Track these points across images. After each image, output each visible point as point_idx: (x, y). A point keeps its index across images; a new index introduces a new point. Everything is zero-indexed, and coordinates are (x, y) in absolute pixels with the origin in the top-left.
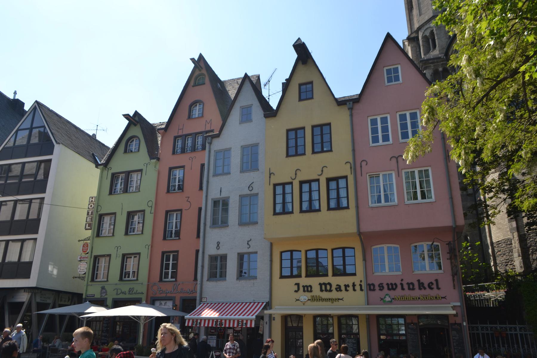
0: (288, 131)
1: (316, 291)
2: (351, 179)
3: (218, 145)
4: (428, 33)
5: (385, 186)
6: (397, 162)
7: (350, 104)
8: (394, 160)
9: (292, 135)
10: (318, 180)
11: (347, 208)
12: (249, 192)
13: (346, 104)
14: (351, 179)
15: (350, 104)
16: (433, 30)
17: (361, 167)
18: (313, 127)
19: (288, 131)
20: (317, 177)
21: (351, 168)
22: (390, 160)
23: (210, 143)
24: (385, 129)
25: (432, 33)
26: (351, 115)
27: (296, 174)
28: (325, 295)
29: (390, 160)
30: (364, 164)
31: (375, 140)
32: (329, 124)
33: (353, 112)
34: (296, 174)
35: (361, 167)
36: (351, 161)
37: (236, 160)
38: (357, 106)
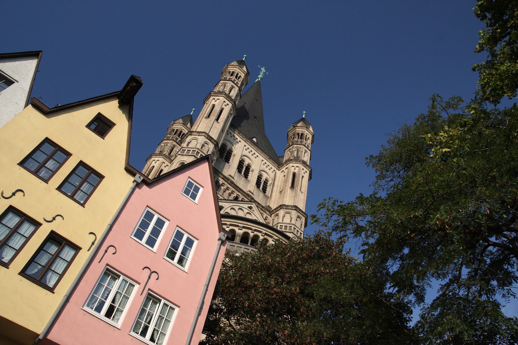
0: (47, 140)
2: (83, 257)
5: (118, 295)
6: (149, 277)
7: (140, 177)
8: (147, 272)
9: (48, 149)
10: (37, 224)
11: (51, 290)
13: (134, 175)
14: (83, 257)
15: (140, 177)
17: (106, 251)
18: (81, 164)
19: (47, 140)
20: (41, 221)
21: (93, 243)
22: (143, 269)
24: (156, 232)
27: (14, 194)
29: (143, 269)
30: (111, 250)
31: (139, 235)
32: (101, 177)
33: (137, 189)
34: (14, 194)
35: (106, 251)
36: (100, 236)
38: (145, 187)
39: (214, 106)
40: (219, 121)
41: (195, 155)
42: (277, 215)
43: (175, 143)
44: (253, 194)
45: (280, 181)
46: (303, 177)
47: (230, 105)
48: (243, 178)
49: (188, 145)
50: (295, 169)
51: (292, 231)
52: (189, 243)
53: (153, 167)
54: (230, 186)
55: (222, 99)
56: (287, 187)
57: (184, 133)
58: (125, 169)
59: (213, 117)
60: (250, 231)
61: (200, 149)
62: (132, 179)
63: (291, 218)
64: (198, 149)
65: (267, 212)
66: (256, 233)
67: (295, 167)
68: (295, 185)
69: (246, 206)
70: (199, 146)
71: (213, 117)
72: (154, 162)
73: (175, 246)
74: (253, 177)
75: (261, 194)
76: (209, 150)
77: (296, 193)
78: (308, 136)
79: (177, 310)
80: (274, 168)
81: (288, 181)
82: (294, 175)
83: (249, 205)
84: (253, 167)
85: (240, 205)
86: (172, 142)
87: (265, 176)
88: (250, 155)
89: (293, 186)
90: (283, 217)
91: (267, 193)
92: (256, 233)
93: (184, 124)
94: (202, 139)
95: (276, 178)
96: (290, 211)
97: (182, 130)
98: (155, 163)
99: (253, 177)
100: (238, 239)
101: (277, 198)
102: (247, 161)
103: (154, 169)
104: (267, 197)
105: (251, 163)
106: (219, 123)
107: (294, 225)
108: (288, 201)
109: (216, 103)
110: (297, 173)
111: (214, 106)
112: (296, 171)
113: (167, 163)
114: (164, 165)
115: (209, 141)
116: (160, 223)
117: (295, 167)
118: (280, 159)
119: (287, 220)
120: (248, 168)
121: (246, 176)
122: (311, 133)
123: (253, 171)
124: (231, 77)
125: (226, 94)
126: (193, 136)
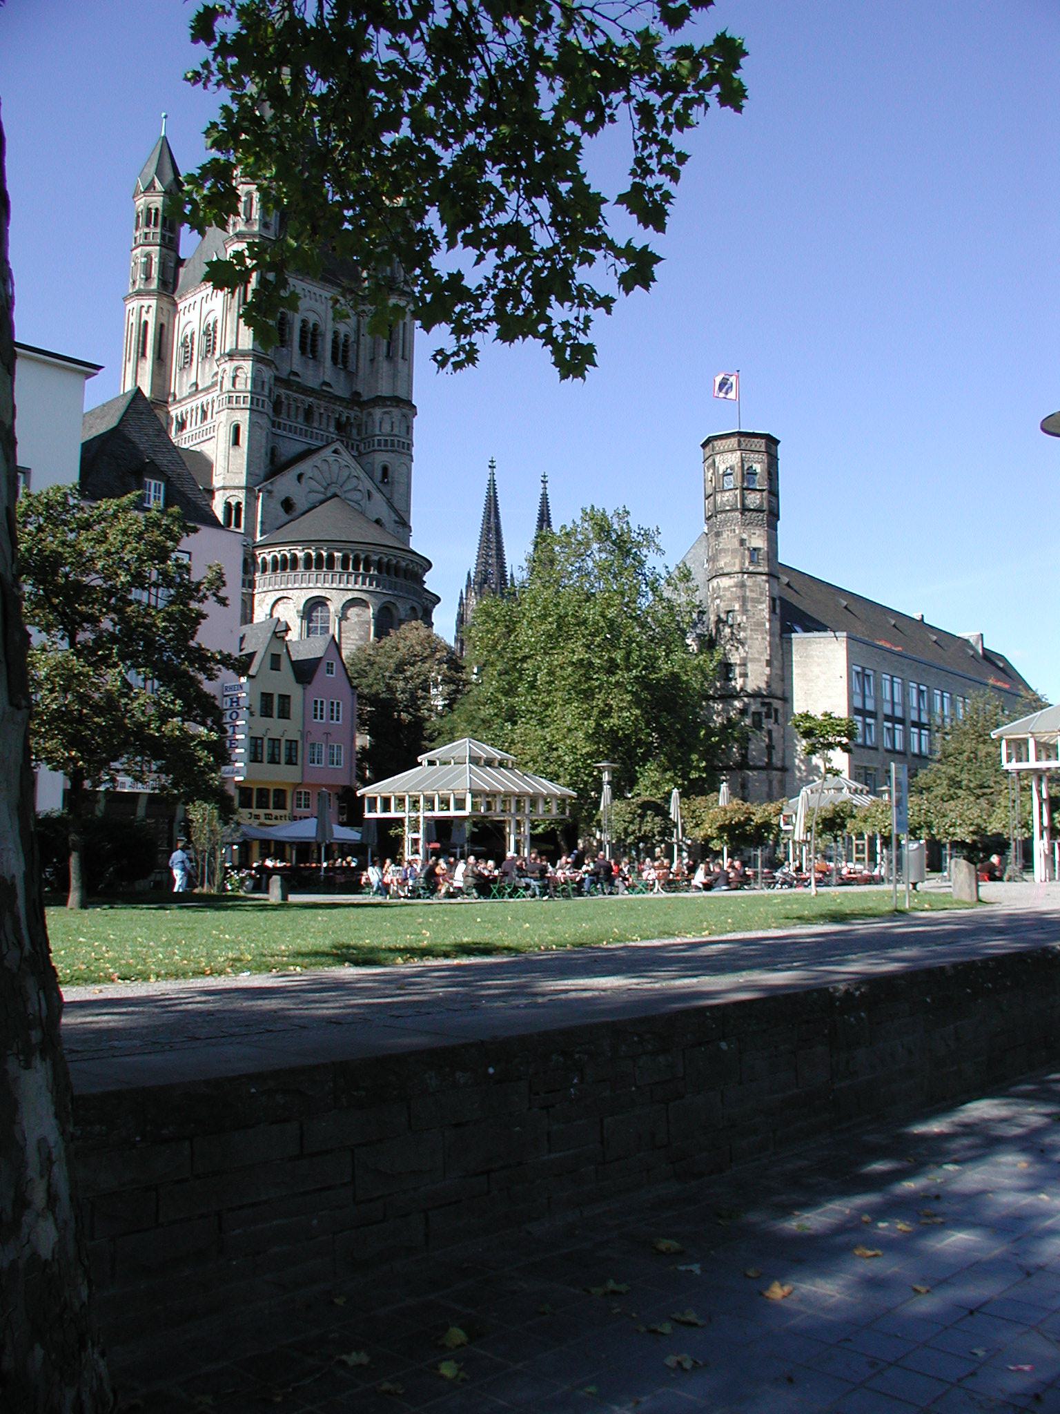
1: (262, 817)
4: (233, 502)
10: (279, 740)
11: (296, 764)
24: (322, 710)
25: (239, 504)
26: (304, 694)
28: (268, 822)
31: (316, 718)
38: (309, 687)
41: (248, 406)
42: (370, 414)
48: (311, 362)
53: (146, 323)
54: (296, 395)
56: (381, 358)
63: (393, 423)
75: (342, 374)
84: (322, 328)
91: (352, 367)
96: (391, 409)
98: (147, 312)
104: (351, 375)
105: (318, 319)
107: (396, 436)
108: (384, 389)
121: (314, 351)
123: (323, 335)
126: (236, 363)
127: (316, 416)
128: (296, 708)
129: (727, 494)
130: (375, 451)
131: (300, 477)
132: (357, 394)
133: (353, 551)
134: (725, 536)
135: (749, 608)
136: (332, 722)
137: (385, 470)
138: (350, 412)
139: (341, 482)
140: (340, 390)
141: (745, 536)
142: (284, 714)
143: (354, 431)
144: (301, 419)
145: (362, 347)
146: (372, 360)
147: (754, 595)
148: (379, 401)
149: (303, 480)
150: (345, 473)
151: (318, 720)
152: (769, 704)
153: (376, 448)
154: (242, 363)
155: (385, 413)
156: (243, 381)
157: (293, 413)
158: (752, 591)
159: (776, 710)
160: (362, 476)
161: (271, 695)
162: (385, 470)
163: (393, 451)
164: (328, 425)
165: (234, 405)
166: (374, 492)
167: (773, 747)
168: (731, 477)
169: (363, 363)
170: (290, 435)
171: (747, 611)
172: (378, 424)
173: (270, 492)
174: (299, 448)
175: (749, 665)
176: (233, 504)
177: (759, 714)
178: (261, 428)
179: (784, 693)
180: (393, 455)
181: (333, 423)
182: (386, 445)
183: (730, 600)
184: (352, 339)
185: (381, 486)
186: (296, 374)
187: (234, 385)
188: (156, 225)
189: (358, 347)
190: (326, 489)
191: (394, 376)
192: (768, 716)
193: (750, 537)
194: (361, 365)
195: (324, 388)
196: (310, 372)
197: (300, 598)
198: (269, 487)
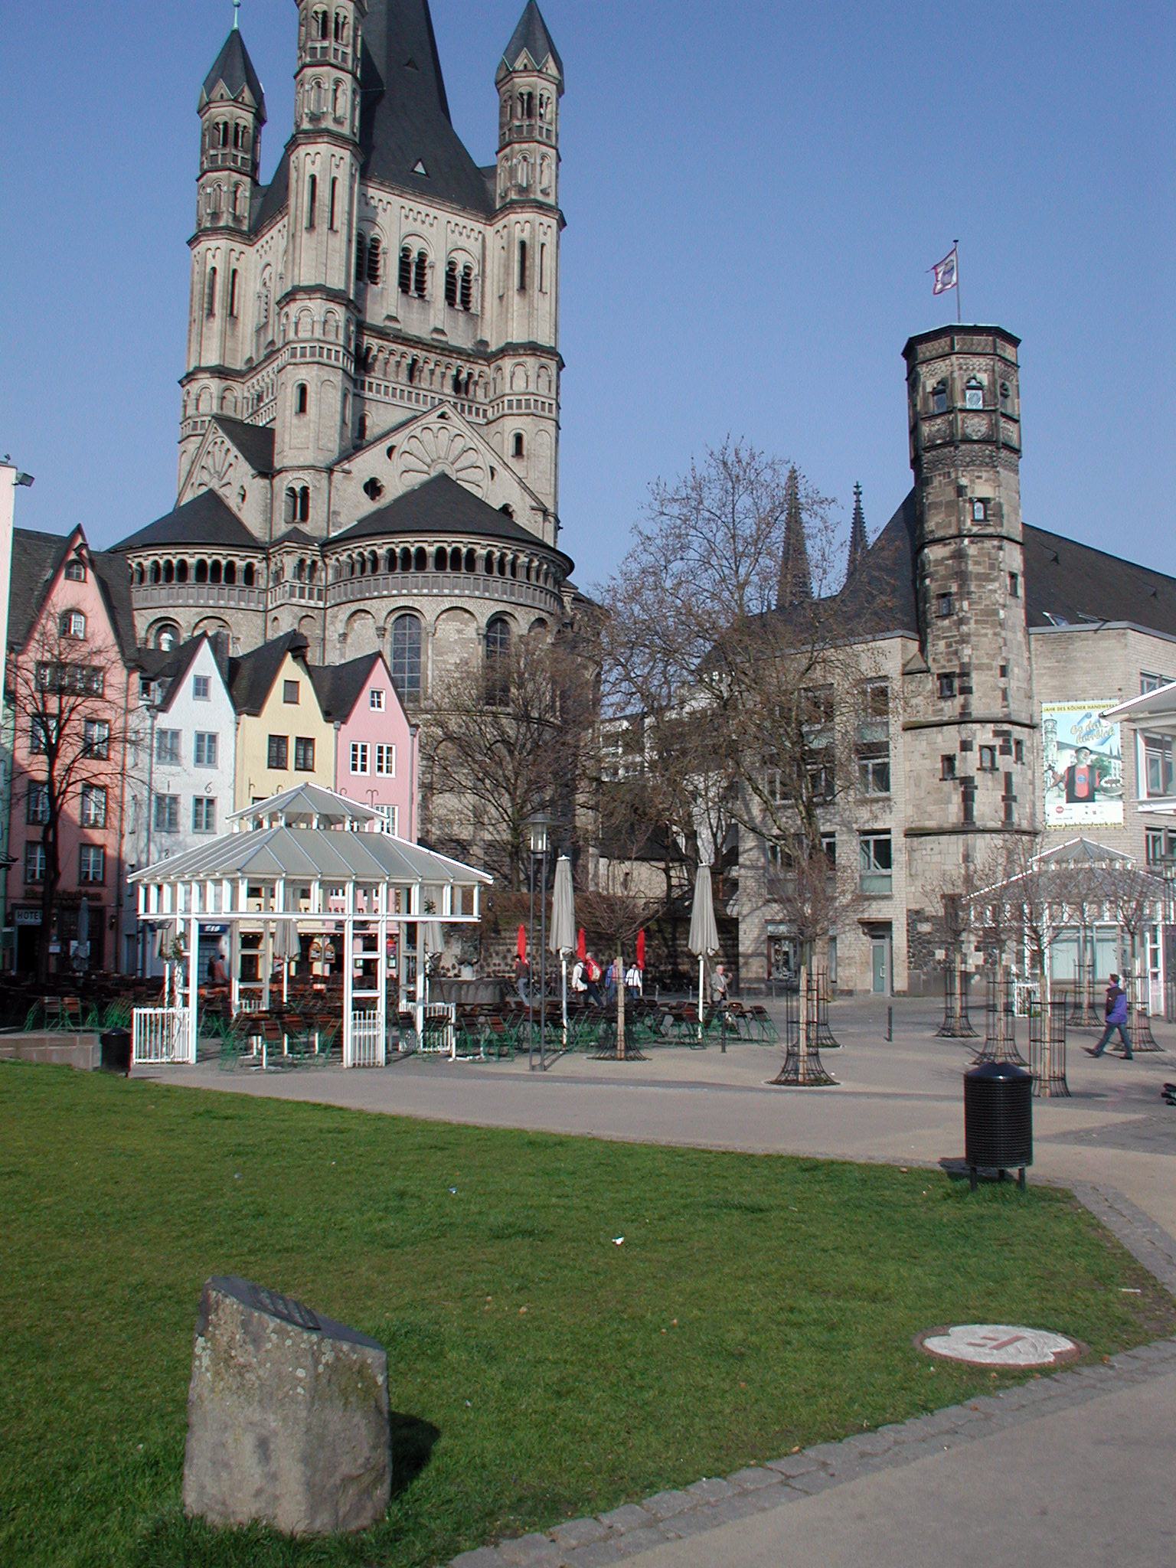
3: (164, 721)
12: (206, 794)
16: (307, 488)
23: (154, 718)
24: (364, 758)
25: (305, 490)
26: (337, 737)
31: (354, 768)
37: (187, 747)
39: (313, 178)
40: (337, 225)
42: (500, 369)
43: (236, 176)
44: (442, 332)
45: (496, 267)
46: (543, 245)
47: (347, 154)
48: (417, 303)
49: (296, 333)
50: (523, 231)
51: (532, 410)
52: (389, 750)
53: (214, 270)
54: (394, 346)
55: (323, 148)
56: (510, 293)
57: (245, 127)
58: (326, 721)
59: (322, 226)
60: (445, 545)
61: (322, 338)
62: (332, 725)
64: (319, 340)
65: (480, 362)
66: (454, 545)
67: (522, 222)
68: (528, 280)
69: (433, 416)
70: (318, 334)
71: (322, 226)
72: (210, 254)
73: (380, 759)
74: (436, 283)
75: (462, 317)
76: (337, 327)
77: (531, 304)
78: (546, 94)
79: (397, 808)
80: (478, 226)
81: (511, 271)
82: (523, 245)
83: (439, 412)
85: (424, 421)
86: (230, 176)
87: (461, 259)
88: (417, 227)
89: (523, 287)
90: (512, 377)
91: (475, 307)
92: (454, 545)
93: (235, 100)
94: (317, 306)
95: (487, 253)
97: (238, 121)
99: (436, 283)
100: (431, 562)
101: (495, 314)
102: (416, 246)
103: (219, 279)
104: (474, 319)
105: (425, 245)
106: (337, 231)
109: (315, 170)
110: (528, 242)
111: (313, 178)
112: (526, 236)
113: (238, 247)
114: (234, 255)
115: (332, 305)
116: (364, 748)
117: (522, 222)
118: (489, 185)
119: (520, 385)
120: (422, 257)
121: (420, 287)
122: (552, 79)
124: (326, 44)
125: (328, 132)
127: (426, 373)
128: (323, 754)
129: (939, 421)
130: (503, 416)
131: (390, 451)
132: (484, 343)
133: (449, 544)
134: (936, 483)
135: (973, 589)
136: (354, 773)
137: (519, 439)
138: (474, 366)
139: (451, 459)
140: (459, 337)
141: (964, 481)
142: (305, 766)
143: (480, 392)
144: (403, 377)
145: (488, 282)
146: (501, 297)
147: (980, 569)
148: (509, 349)
149: (395, 455)
150: (459, 443)
151: (359, 772)
152: (1007, 733)
153: (507, 411)
154: (308, 303)
155: (519, 364)
156: (309, 327)
157: (391, 368)
158: (977, 563)
159: (1019, 743)
160: (481, 447)
161: (284, 739)
162: (519, 439)
163: (528, 415)
164: (442, 386)
165: (298, 360)
166: (499, 469)
167: (1014, 799)
168: (944, 395)
169: (491, 302)
170: (387, 399)
171: (969, 593)
172: (508, 380)
173: (348, 472)
174: (401, 416)
175: (974, 675)
176: (298, 489)
177: (991, 749)
178: (334, 387)
179: (1031, 717)
180: (529, 419)
181: (449, 383)
182: (519, 407)
183: (945, 578)
184: (475, 272)
185: (511, 462)
186: (394, 319)
187: (296, 333)
188: (225, 144)
189: (483, 281)
190: (429, 466)
191: (530, 315)
192: (1005, 750)
193: (972, 481)
194: (487, 305)
195: (435, 336)
196: (415, 316)
197: (381, 608)
198: (346, 467)
